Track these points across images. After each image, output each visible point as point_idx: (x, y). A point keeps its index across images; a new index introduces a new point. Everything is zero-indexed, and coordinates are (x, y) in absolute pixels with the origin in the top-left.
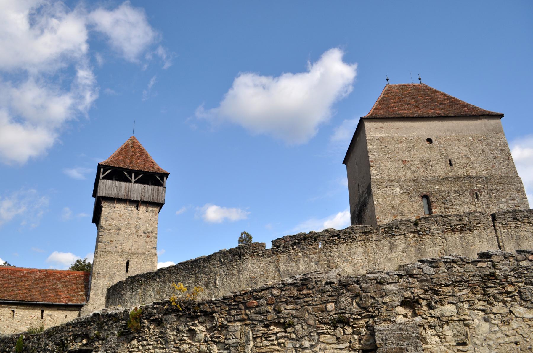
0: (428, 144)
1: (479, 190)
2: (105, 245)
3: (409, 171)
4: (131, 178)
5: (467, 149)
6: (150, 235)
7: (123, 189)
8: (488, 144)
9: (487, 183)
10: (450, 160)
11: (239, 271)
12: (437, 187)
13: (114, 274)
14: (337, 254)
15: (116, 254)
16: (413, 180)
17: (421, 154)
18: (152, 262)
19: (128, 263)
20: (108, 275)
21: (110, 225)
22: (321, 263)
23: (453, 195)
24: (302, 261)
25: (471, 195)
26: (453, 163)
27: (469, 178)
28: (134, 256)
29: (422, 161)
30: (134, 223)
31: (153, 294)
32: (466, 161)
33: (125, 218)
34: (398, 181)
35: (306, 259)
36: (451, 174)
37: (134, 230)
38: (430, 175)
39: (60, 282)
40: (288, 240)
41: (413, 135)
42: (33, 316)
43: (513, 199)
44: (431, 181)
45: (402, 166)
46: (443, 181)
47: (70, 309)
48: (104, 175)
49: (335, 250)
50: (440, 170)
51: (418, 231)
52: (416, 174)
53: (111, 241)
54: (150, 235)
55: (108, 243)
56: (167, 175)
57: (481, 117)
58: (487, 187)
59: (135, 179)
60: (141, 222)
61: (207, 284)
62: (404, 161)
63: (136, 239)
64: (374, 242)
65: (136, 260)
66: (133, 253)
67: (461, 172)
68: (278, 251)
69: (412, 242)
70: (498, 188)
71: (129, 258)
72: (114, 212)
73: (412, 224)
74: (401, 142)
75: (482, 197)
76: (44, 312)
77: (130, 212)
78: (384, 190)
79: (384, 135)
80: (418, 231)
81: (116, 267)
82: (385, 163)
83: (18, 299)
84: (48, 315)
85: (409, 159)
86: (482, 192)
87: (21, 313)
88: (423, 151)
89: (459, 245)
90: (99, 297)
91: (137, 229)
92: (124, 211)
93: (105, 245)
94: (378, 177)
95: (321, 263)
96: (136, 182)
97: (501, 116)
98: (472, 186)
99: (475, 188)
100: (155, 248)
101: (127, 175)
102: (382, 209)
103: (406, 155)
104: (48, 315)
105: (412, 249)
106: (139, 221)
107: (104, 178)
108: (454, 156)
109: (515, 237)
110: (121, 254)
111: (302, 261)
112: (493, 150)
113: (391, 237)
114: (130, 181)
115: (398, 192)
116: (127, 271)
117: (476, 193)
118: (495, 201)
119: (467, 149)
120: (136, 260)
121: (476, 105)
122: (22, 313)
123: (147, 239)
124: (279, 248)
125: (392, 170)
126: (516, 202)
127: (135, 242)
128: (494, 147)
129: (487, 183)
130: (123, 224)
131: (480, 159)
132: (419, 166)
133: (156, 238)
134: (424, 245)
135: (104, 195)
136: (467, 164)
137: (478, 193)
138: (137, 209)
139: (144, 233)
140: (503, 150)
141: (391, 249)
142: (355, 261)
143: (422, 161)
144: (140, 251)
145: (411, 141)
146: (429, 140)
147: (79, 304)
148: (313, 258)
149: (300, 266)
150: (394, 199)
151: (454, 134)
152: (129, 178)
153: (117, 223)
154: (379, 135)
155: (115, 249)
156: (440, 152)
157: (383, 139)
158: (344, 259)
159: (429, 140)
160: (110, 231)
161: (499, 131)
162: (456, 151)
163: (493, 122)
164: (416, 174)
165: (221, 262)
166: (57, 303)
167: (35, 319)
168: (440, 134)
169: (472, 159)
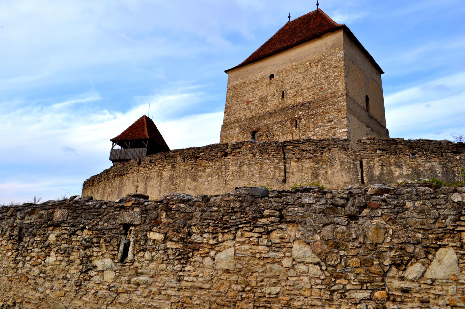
1: (300, 118)
3: (249, 111)
10: (283, 92)
23: (275, 127)
32: (297, 88)
43: (330, 121)
50: (273, 103)
52: (253, 113)
58: (308, 113)
62: (248, 102)
70: (318, 112)
75: (301, 124)
86: (302, 119)
98: (294, 115)
99: (296, 116)
103: (250, 96)
109: (145, 178)
115: (236, 132)
117: (296, 121)
118: (312, 126)
126: (333, 123)
128: (327, 67)
131: (311, 83)
136: (297, 92)
137: (298, 120)
140: (337, 67)
145: (258, 81)
156: (277, 86)
162: (291, 81)
164: (253, 113)
168: (282, 67)
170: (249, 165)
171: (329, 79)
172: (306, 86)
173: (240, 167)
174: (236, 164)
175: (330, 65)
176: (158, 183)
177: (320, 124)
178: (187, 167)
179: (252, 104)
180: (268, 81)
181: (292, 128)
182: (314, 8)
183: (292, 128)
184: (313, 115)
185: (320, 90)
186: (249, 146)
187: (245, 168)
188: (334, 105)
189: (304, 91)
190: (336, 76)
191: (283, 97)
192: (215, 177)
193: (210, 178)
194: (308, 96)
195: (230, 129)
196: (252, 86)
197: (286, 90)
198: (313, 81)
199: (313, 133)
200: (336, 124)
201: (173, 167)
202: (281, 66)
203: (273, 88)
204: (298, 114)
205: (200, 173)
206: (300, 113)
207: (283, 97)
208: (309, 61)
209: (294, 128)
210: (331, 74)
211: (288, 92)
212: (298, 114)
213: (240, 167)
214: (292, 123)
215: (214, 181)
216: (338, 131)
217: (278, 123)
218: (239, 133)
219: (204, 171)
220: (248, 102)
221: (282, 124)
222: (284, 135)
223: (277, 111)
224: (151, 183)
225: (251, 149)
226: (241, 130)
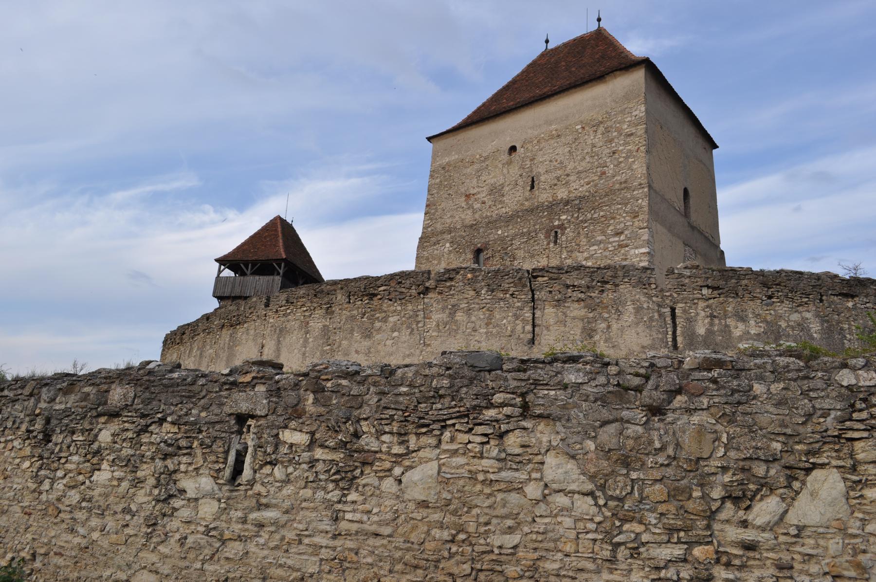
1: (562, 227)
3: (469, 212)
10: (533, 178)
17: (494, 177)
23: (517, 243)
32: (559, 172)
50: (515, 199)
52: (477, 216)
57: (608, 78)
62: (468, 196)
70: (596, 216)
75: (564, 238)
82: (443, 205)
86: (566, 228)
98: (551, 220)
99: (556, 223)
103: (471, 186)
109: (278, 331)
115: (446, 250)
117: (556, 232)
118: (584, 241)
126: (622, 237)
128: (615, 134)
131: (583, 164)
136: (558, 179)
137: (559, 231)
140: (632, 134)
145: (486, 158)
156: (522, 167)
164: (477, 216)
170: (468, 311)
171: (616, 156)
172: (575, 168)
173: (452, 314)
174: (444, 309)
175: (620, 131)
176: (301, 341)
177: (599, 238)
178: (355, 312)
179: (476, 200)
180: (505, 157)
181: (548, 244)
182: (593, 27)
183: (548, 244)
184: (586, 221)
185: (600, 177)
186: (469, 276)
187: (460, 316)
188: (626, 204)
189: (572, 178)
190: (630, 151)
191: (532, 187)
192: (405, 332)
193: (396, 334)
194: (578, 187)
195: (435, 244)
196: (476, 166)
197: (539, 174)
198: (588, 159)
199: (585, 255)
200: (629, 239)
201: (329, 311)
202: (530, 131)
203: (515, 170)
204: (559, 220)
205: (378, 324)
206: (564, 217)
207: (532, 187)
208: (582, 122)
209: (552, 245)
210: (621, 148)
211: (542, 178)
212: (559, 220)
213: (452, 314)
214: (547, 236)
215: (404, 338)
216: (632, 252)
218: (450, 252)
219: (385, 320)
220: (468, 196)
221: (530, 236)
222: (532, 256)
223: (520, 214)
224: (288, 340)
225: (471, 282)
226: (455, 246)
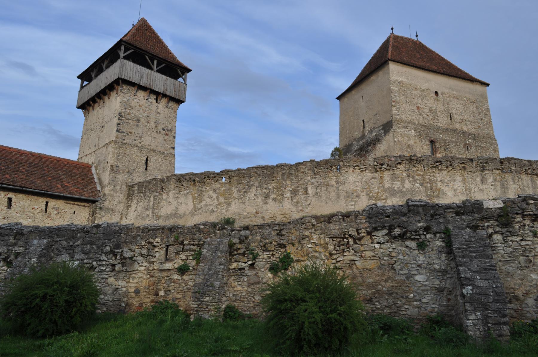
0: (435, 97)
2: (125, 136)
4: (153, 65)
5: (463, 108)
6: (169, 133)
7: (145, 76)
8: (477, 107)
9: (475, 140)
11: (337, 182)
12: (441, 136)
13: (134, 170)
14: (439, 179)
15: (136, 148)
16: (424, 126)
17: (431, 104)
18: (170, 163)
19: (147, 160)
20: (127, 170)
21: (129, 114)
22: (426, 185)
23: (452, 145)
24: (407, 181)
25: (464, 147)
26: (453, 118)
27: (464, 133)
28: (154, 154)
29: (431, 110)
30: (153, 116)
31: (215, 196)
32: (462, 118)
33: (144, 109)
34: (413, 124)
35: (411, 179)
36: (451, 127)
37: (153, 124)
38: (436, 124)
39: (61, 171)
40: (393, 159)
41: (425, 86)
42: (36, 207)
44: (437, 129)
45: (416, 111)
46: (445, 131)
47: (79, 203)
48: (126, 54)
49: (438, 175)
50: (443, 122)
51: (503, 169)
52: (426, 121)
53: (131, 133)
54: (169, 133)
55: (127, 134)
56: (189, 71)
59: (157, 67)
60: (161, 117)
61: (294, 192)
62: (418, 107)
63: (156, 135)
64: (469, 173)
65: (155, 158)
66: (154, 151)
67: (458, 126)
68: (381, 168)
69: (498, 177)
71: (149, 155)
72: (133, 100)
73: (498, 163)
74: (416, 89)
75: (471, 151)
76: (49, 204)
77: (149, 104)
78: (403, 130)
79: (404, 80)
80: (503, 169)
81: (136, 163)
82: (404, 105)
83: (19, 184)
84: (54, 208)
85: (422, 106)
87: (20, 201)
88: (430, 102)
89: (530, 186)
90: (118, 194)
91: (157, 124)
92: (143, 101)
93: (125, 136)
94: (398, 117)
95: (426, 185)
96: (158, 71)
97: (488, 85)
98: (465, 140)
100: (173, 148)
101: (149, 61)
102: (400, 146)
104: (54, 208)
105: (498, 184)
106: (158, 115)
107: (125, 58)
108: (454, 111)
110: (141, 149)
111: (407, 181)
112: (480, 113)
113: (482, 171)
114: (151, 69)
115: (413, 134)
116: (146, 169)
119: (463, 108)
120: (155, 158)
121: (467, 71)
122: (21, 203)
123: (166, 137)
124: (384, 166)
125: (409, 113)
127: (155, 138)
129: (475, 140)
130: (142, 115)
132: (428, 114)
133: (174, 137)
134: (506, 182)
135: (126, 78)
138: (157, 102)
139: (164, 130)
141: (483, 181)
142: (456, 187)
143: (431, 110)
144: (159, 149)
145: (423, 91)
146: (436, 93)
147: (92, 199)
148: (417, 179)
149: (405, 185)
150: (409, 140)
151: (454, 92)
152: (151, 64)
153: (137, 114)
154: (400, 79)
155: (134, 142)
157: (403, 84)
158: (446, 184)
159: (436, 93)
160: (130, 121)
161: (484, 97)
163: (479, 88)
165: (314, 172)
166: (68, 195)
167: (38, 211)
168: (445, 90)
169: (466, 117)
175: (482, 111)
217: (454, 142)
220: (418, 107)
226: (418, 134)
